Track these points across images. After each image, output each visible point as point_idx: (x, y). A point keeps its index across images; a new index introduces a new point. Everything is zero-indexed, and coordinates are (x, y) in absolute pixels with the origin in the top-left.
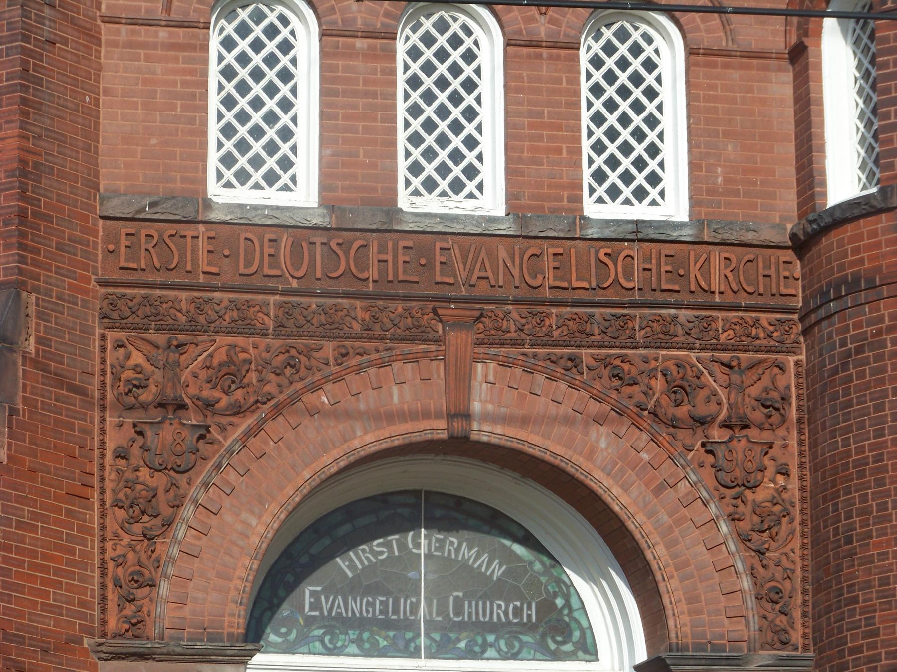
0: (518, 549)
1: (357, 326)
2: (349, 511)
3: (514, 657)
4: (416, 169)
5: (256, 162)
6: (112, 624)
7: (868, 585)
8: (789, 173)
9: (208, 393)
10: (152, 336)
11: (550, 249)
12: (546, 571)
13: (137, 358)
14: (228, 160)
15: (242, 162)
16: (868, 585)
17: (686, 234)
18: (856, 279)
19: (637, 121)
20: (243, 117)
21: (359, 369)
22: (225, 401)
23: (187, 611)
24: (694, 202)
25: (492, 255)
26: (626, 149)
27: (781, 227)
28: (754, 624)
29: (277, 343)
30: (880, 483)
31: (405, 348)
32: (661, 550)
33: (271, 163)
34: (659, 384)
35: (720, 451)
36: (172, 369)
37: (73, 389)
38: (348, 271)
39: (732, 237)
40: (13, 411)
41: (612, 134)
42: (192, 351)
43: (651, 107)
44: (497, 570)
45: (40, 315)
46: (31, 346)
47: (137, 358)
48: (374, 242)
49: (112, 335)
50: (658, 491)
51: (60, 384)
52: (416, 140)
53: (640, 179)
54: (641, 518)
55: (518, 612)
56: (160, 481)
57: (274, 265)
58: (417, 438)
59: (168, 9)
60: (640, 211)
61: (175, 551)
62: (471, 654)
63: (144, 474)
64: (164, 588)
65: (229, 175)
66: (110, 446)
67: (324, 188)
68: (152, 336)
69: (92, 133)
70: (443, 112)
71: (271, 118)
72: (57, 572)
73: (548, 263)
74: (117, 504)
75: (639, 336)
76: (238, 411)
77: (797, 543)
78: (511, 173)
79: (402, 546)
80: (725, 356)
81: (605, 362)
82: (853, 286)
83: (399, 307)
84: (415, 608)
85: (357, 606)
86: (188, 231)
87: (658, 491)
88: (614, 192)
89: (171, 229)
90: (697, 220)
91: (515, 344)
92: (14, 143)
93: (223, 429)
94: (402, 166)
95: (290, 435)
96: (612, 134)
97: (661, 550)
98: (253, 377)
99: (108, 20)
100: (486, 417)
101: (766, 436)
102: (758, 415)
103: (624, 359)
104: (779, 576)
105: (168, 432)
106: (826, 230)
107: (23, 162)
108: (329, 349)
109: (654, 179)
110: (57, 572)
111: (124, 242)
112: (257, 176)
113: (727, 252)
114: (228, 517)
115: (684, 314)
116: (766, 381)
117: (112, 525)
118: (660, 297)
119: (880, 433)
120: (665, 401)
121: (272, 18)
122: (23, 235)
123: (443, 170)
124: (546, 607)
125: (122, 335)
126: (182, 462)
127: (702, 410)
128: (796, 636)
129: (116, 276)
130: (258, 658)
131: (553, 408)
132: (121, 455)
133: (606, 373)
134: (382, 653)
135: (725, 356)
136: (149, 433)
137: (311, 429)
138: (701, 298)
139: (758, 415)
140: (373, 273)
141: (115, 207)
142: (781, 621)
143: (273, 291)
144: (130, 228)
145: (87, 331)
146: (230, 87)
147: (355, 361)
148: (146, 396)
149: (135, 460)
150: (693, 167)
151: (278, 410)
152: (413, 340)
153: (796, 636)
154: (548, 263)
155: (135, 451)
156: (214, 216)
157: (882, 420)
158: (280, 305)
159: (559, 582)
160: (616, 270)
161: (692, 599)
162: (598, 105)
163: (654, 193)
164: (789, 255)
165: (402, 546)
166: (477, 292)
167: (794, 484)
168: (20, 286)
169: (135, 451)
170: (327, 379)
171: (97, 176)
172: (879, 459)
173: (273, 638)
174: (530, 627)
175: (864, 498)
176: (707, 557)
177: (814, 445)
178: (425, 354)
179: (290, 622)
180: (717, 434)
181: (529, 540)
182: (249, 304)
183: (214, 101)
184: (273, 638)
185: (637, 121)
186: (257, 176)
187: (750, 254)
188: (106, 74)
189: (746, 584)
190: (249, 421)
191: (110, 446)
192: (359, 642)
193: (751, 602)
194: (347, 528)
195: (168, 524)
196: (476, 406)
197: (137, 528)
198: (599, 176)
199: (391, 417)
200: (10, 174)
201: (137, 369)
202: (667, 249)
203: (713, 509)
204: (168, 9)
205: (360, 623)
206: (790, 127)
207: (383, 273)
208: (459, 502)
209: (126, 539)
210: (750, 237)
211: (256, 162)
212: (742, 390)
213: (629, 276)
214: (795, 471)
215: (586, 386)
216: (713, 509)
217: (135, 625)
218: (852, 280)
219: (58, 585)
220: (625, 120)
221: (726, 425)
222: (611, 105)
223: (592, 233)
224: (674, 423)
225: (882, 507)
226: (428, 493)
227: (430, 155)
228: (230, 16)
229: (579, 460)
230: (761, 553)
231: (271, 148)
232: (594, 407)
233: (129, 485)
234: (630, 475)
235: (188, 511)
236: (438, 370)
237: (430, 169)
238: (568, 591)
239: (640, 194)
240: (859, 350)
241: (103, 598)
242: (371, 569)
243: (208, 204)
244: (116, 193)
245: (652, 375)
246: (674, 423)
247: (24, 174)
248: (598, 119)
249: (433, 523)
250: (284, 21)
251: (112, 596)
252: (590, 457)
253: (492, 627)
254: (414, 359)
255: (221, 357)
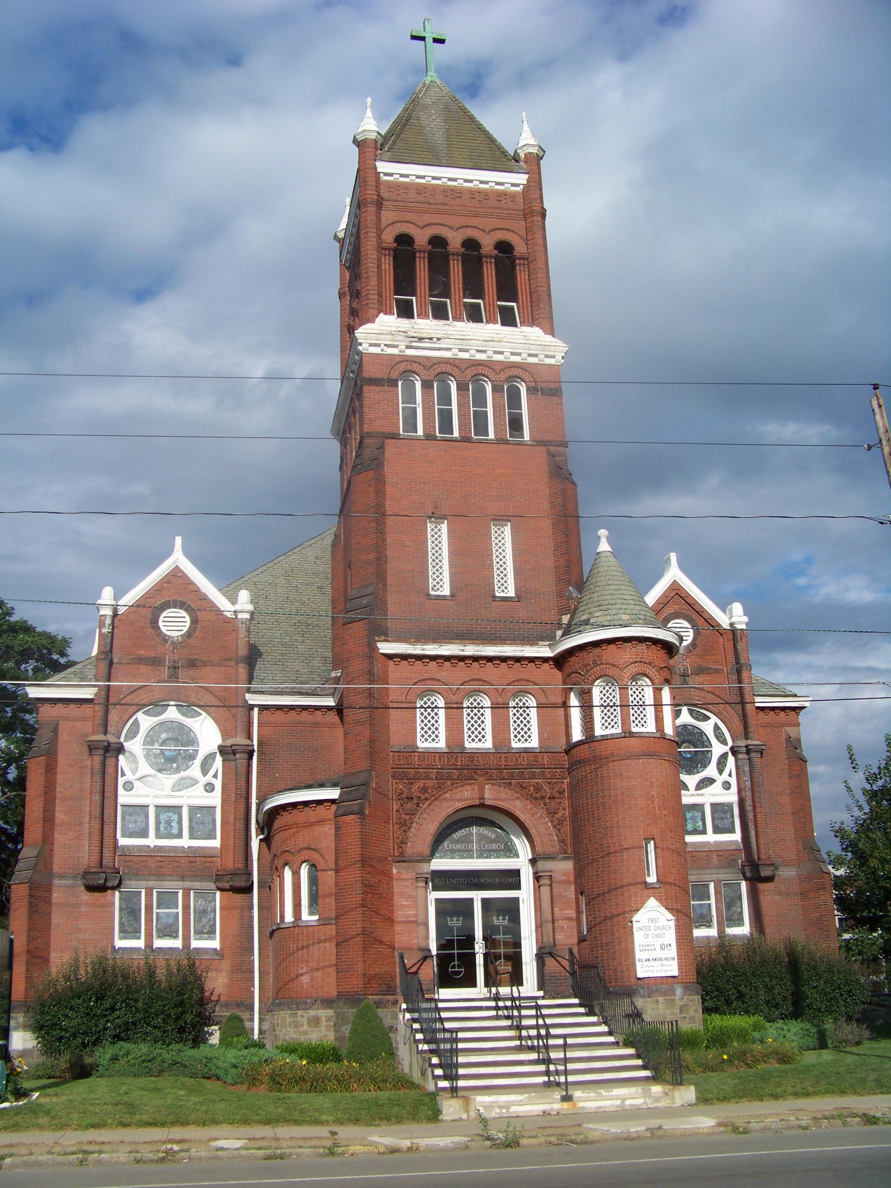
0: (499, 830)
1: (456, 777)
2: (456, 822)
3: (498, 858)
4: (470, 736)
5: (430, 736)
6: (396, 853)
7: (586, 838)
8: (563, 733)
9: (419, 795)
10: (404, 781)
11: (504, 756)
12: (506, 836)
13: (401, 787)
14: (423, 736)
15: (426, 736)
16: (586, 838)
17: (538, 750)
18: (580, 760)
19: (525, 722)
20: (426, 725)
21: (456, 787)
22: (423, 797)
23: (415, 850)
24: (540, 742)
25: (489, 758)
26: (522, 729)
27: (562, 747)
28: (558, 847)
29: (436, 782)
30: (588, 812)
31: (468, 782)
32: (534, 830)
33: (433, 736)
34: (532, 788)
35: (548, 805)
36: (410, 789)
37: (385, 795)
38: (453, 763)
39: (550, 751)
40: (370, 801)
41: (519, 726)
42: (415, 784)
43: (528, 718)
44: (493, 836)
45: (376, 777)
46: (374, 785)
47: (401, 787)
48: (459, 755)
49: (394, 781)
50: (533, 815)
51: (381, 794)
52: (469, 729)
53: (526, 736)
54: (528, 822)
55: (499, 847)
56: (407, 817)
57: (435, 762)
58: (472, 804)
59: (406, 699)
60: (526, 745)
61: (412, 835)
62: (487, 857)
63: (403, 816)
64: (409, 844)
65: (423, 740)
66: (395, 808)
67: (447, 742)
68: (404, 781)
69: (388, 731)
70: (476, 722)
71: (433, 725)
72: (382, 841)
73: (503, 759)
74: (397, 823)
75: (527, 776)
76: (426, 799)
77: (568, 827)
78: (493, 736)
79: (469, 831)
80: (549, 781)
81: (518, 783)
82: (580, 762)
83: (466, 771)
84: (473, 846)
85: (459, 846)
86: (413, 754)
87: (533, 815)
88: (519, 740)
89: (409, 754)
90: (540, 747)
91: (495, 780)
92: (368, 734)
93: (423, 804)
94: (466, 736)
95: (439, 805)
96: (519, 726)
97: (534, 830)
98: (430, 790)
99: (391, 702)
100: (488, 799)
101: (559, 801)
102: (557, 795)
103: (523, 782)
104: (564, 835)
105: (409, 805)
106: (573, 748)
107: (371, 739)
108: (449, 782)
109: (529, 736)
110: (382, 841)
111: (397, 757)
112: (430, 740)
113: (548, 754)
114: (424, 826)
115: (538, 770)
116: (559, 786)
117: (395, 829)
118: (532, 766)
119: (587, 799)
120: (534, 792)
121: (432, 700)
122: (371, 757)
123: (476, 736)
124: (506, 845)
125: (397, 781)
126: (413, 813)
127: (543, 795)
128: (569, 851)
129: (395, 766)
130: (433, 860)
131: (505, 796)
132: (397, 811)
133: (519, 786)
134: (465, 858)
135: (549, 781)
136: (404, 805)
137: (445, 804)
138: (542, 766)
139: (557, 795)
140: (459, 763)
141: (394, 749)
142: (565, 847)
143: (434, 769)
144: (398, 754)
145: (388, 780)
146: (422, 718)
147: (455, 785)
148: (403, 796)
149: (401, 812)
150: (539, 733)
151: (436, 799)
152: (470, 780)
153: (569, 851)
154: (503, 759)
155: (401, 810)
156: (419, 750)
157: (588, 796)
158: (436, 772)
159: (509, 838)
160: (520, 760)
161: (542, 842)
162: (515, 718)
163: (529, 740)
164: (564, 754)
165: (469, 831)
166: (486, 767)
167: (567, 813)
168: (371, 770)
169: (401, 810)
170: (448, 790)
171: (389, 740)
172: (587, 806)
173: (437, 855)
174: (502, 850)
175: (584, 816)
176: (545, 831)
177: (571, 802)
178: (473, 783)
179: (442, 851)
180: (547, 801)
181: (501, 828)
182: (428, 772)
183: (418, 721)
184: (437, 855)
185: (525, 722)
186: (430, 740)
187: (554, 754)
188: (391, 715)
189: (555, 838)
190: (428, 802)
191: (395, 808)
192: (459, 855)
193: (557, 843)
194: (455, 827)
195: (410, 828)
196: (486, 796)
197: (402, 829)
198: (516, 736)
199: (465, 800)
200: (367, 742)
201: (401, 789)
202: (534, 754)
203: (546, 819)
204: (406, 699)
205: (459, 851)
206: (563, 722)
207: (462, 763)
208: (483, 819)
209: (399, 832)
210: (554, 750)
211: (430, 736)
212: (553, 789)
213: (523, 761)
214: (567, 809)
215: (513, 790)
216: (546, 819)
217: (402, 854)
218: (495, 939)
219: (382, 844)
220: (522, 722)
221: (549, 798)
222: (518, 718)
223: (514, 751)
224: (536, 799)
225: (589, 818)
226: (476, 817)
227: (473, 733)
228: (422, 700)
229: (512, 808)
230: (559, 830)
231: (433, 733)
232: (516, 795)
233: (400, 818)
234: (525, 812)
235: (414, 825)
236: (476, 787)
237: (473, 736)
238: (511, 841)
239: (526, 740)
240: (582, 778)
241: (394, 847)
242: (461, 837)
243: (418, 748)
244: (394, 745)
245: (530, 786)
246: (536, 799)
247: (371, 742)
248: (515, 722)
249: (478, 825)
250: (436, 700)
251: (396, 846)
252: (515, 807)
253: (492, 850)
254: (470, 784)
255: (422, 785)
